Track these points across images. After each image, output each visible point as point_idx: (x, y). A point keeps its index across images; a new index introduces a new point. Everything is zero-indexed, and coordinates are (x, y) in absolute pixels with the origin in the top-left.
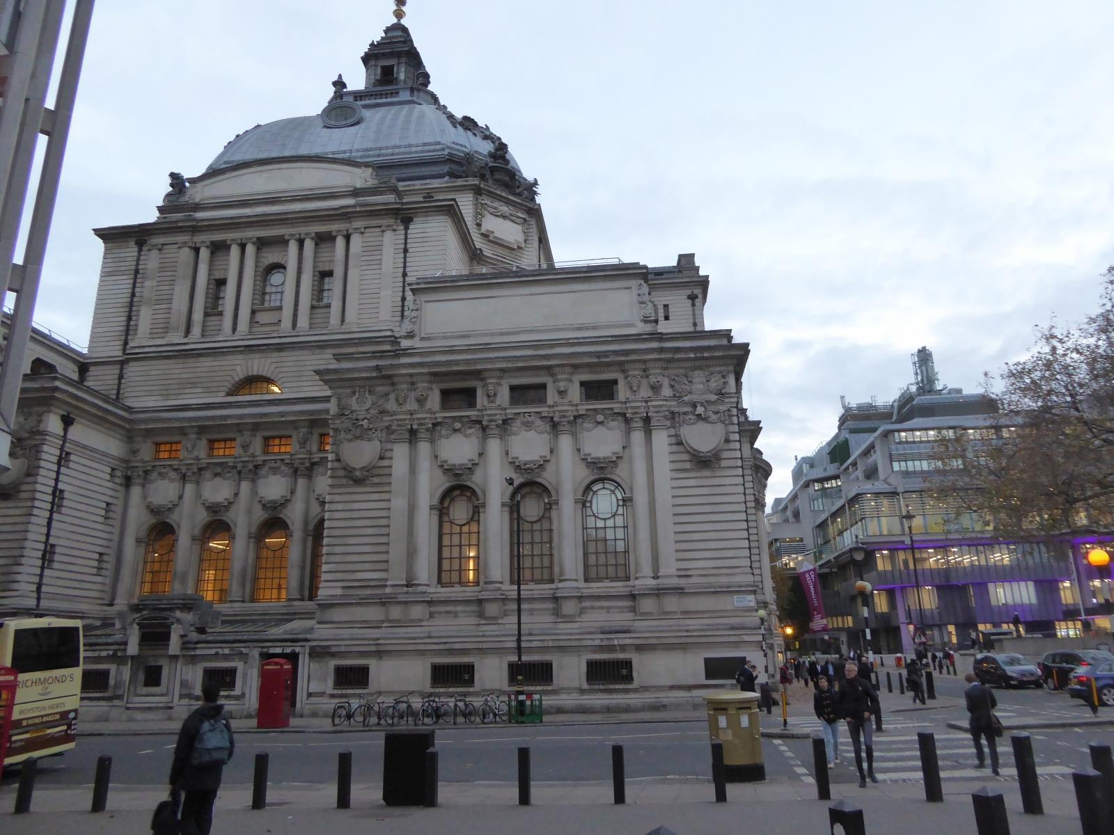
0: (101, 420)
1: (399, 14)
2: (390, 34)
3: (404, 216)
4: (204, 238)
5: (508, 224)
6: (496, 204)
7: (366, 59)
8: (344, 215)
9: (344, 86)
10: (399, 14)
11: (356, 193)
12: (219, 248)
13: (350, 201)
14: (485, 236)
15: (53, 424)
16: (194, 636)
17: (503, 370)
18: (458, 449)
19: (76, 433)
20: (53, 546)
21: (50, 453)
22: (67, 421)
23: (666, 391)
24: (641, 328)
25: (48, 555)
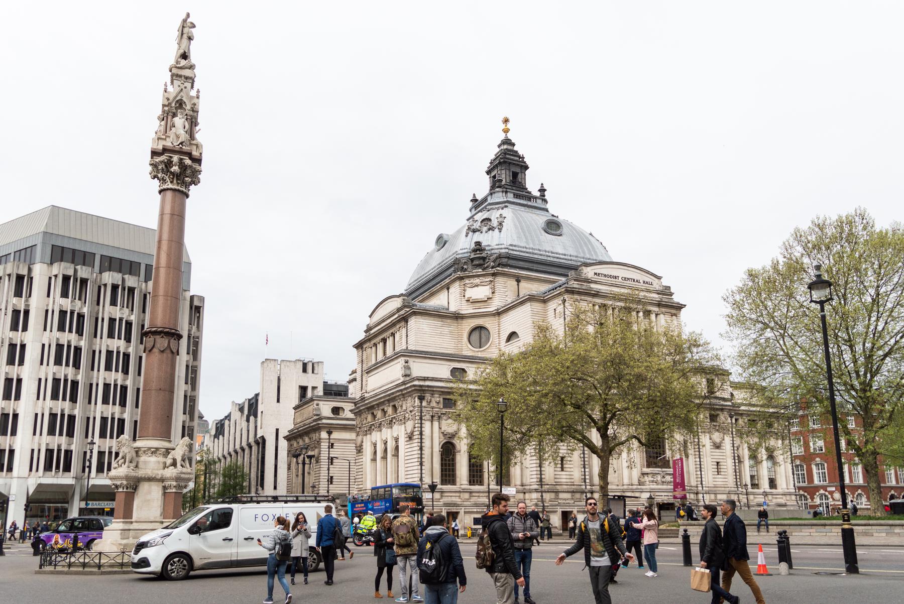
0: (345, 428)
1: (506, 131)
2: (502, 147)
3: (405, 319)
4: (373, 342)
5: (480, 287)
6: (472, 281)
7: (488, 173)
8: (393, 325)
9: (476, 200)
10: (506, 131)
11: (399, 310)
12: (375, 345)
13: (396, 316)
14: (468, 301)
15: (324, 435)
16: (340, 508)
17: (377, 405)
18: (376, 436)
19: (332, 436)
20: (332, 477)
21: (324, 445)
22: (330, 433)
23: (404, 408)
24: (402, 379)
25: (331, 480)
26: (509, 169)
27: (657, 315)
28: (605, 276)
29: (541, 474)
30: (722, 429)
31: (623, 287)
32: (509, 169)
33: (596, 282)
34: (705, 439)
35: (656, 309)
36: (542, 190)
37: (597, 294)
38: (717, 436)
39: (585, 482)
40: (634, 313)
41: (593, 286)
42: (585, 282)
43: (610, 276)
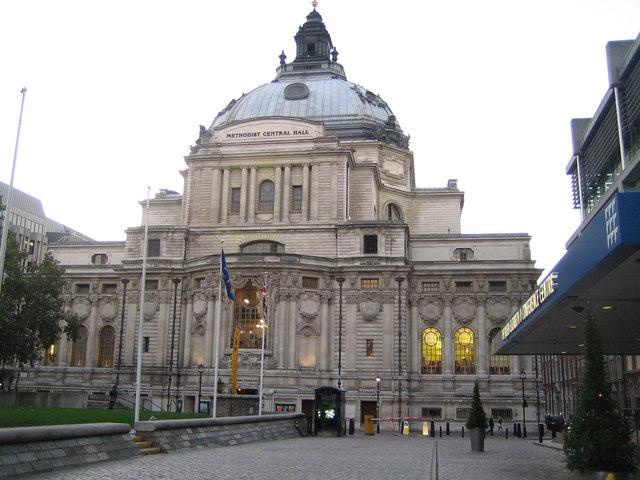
26: (314, 45)
27: (310, 168)
28: (241, 135)
29: (120, 355)
30: (383, 299)
31: (264, 143)
32: (314, 45)
33: (228, 145)
34: (351, 314)
35: (308, 160)
36: (335, 54)
37: (222, 158)
38: (369, 307)
39: (172, 363)
40: (278, 170)
41: (223, 150)
42: (213, 147)
43: (248, 135)
